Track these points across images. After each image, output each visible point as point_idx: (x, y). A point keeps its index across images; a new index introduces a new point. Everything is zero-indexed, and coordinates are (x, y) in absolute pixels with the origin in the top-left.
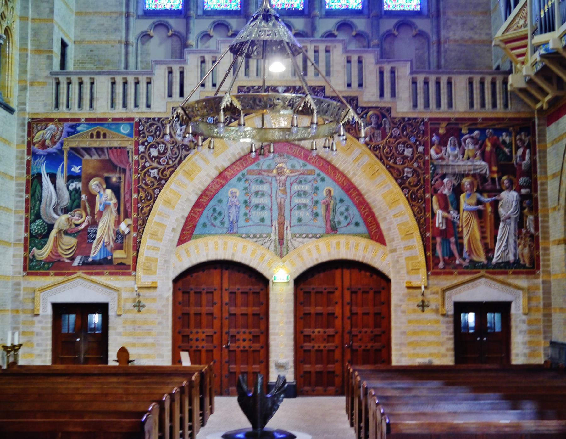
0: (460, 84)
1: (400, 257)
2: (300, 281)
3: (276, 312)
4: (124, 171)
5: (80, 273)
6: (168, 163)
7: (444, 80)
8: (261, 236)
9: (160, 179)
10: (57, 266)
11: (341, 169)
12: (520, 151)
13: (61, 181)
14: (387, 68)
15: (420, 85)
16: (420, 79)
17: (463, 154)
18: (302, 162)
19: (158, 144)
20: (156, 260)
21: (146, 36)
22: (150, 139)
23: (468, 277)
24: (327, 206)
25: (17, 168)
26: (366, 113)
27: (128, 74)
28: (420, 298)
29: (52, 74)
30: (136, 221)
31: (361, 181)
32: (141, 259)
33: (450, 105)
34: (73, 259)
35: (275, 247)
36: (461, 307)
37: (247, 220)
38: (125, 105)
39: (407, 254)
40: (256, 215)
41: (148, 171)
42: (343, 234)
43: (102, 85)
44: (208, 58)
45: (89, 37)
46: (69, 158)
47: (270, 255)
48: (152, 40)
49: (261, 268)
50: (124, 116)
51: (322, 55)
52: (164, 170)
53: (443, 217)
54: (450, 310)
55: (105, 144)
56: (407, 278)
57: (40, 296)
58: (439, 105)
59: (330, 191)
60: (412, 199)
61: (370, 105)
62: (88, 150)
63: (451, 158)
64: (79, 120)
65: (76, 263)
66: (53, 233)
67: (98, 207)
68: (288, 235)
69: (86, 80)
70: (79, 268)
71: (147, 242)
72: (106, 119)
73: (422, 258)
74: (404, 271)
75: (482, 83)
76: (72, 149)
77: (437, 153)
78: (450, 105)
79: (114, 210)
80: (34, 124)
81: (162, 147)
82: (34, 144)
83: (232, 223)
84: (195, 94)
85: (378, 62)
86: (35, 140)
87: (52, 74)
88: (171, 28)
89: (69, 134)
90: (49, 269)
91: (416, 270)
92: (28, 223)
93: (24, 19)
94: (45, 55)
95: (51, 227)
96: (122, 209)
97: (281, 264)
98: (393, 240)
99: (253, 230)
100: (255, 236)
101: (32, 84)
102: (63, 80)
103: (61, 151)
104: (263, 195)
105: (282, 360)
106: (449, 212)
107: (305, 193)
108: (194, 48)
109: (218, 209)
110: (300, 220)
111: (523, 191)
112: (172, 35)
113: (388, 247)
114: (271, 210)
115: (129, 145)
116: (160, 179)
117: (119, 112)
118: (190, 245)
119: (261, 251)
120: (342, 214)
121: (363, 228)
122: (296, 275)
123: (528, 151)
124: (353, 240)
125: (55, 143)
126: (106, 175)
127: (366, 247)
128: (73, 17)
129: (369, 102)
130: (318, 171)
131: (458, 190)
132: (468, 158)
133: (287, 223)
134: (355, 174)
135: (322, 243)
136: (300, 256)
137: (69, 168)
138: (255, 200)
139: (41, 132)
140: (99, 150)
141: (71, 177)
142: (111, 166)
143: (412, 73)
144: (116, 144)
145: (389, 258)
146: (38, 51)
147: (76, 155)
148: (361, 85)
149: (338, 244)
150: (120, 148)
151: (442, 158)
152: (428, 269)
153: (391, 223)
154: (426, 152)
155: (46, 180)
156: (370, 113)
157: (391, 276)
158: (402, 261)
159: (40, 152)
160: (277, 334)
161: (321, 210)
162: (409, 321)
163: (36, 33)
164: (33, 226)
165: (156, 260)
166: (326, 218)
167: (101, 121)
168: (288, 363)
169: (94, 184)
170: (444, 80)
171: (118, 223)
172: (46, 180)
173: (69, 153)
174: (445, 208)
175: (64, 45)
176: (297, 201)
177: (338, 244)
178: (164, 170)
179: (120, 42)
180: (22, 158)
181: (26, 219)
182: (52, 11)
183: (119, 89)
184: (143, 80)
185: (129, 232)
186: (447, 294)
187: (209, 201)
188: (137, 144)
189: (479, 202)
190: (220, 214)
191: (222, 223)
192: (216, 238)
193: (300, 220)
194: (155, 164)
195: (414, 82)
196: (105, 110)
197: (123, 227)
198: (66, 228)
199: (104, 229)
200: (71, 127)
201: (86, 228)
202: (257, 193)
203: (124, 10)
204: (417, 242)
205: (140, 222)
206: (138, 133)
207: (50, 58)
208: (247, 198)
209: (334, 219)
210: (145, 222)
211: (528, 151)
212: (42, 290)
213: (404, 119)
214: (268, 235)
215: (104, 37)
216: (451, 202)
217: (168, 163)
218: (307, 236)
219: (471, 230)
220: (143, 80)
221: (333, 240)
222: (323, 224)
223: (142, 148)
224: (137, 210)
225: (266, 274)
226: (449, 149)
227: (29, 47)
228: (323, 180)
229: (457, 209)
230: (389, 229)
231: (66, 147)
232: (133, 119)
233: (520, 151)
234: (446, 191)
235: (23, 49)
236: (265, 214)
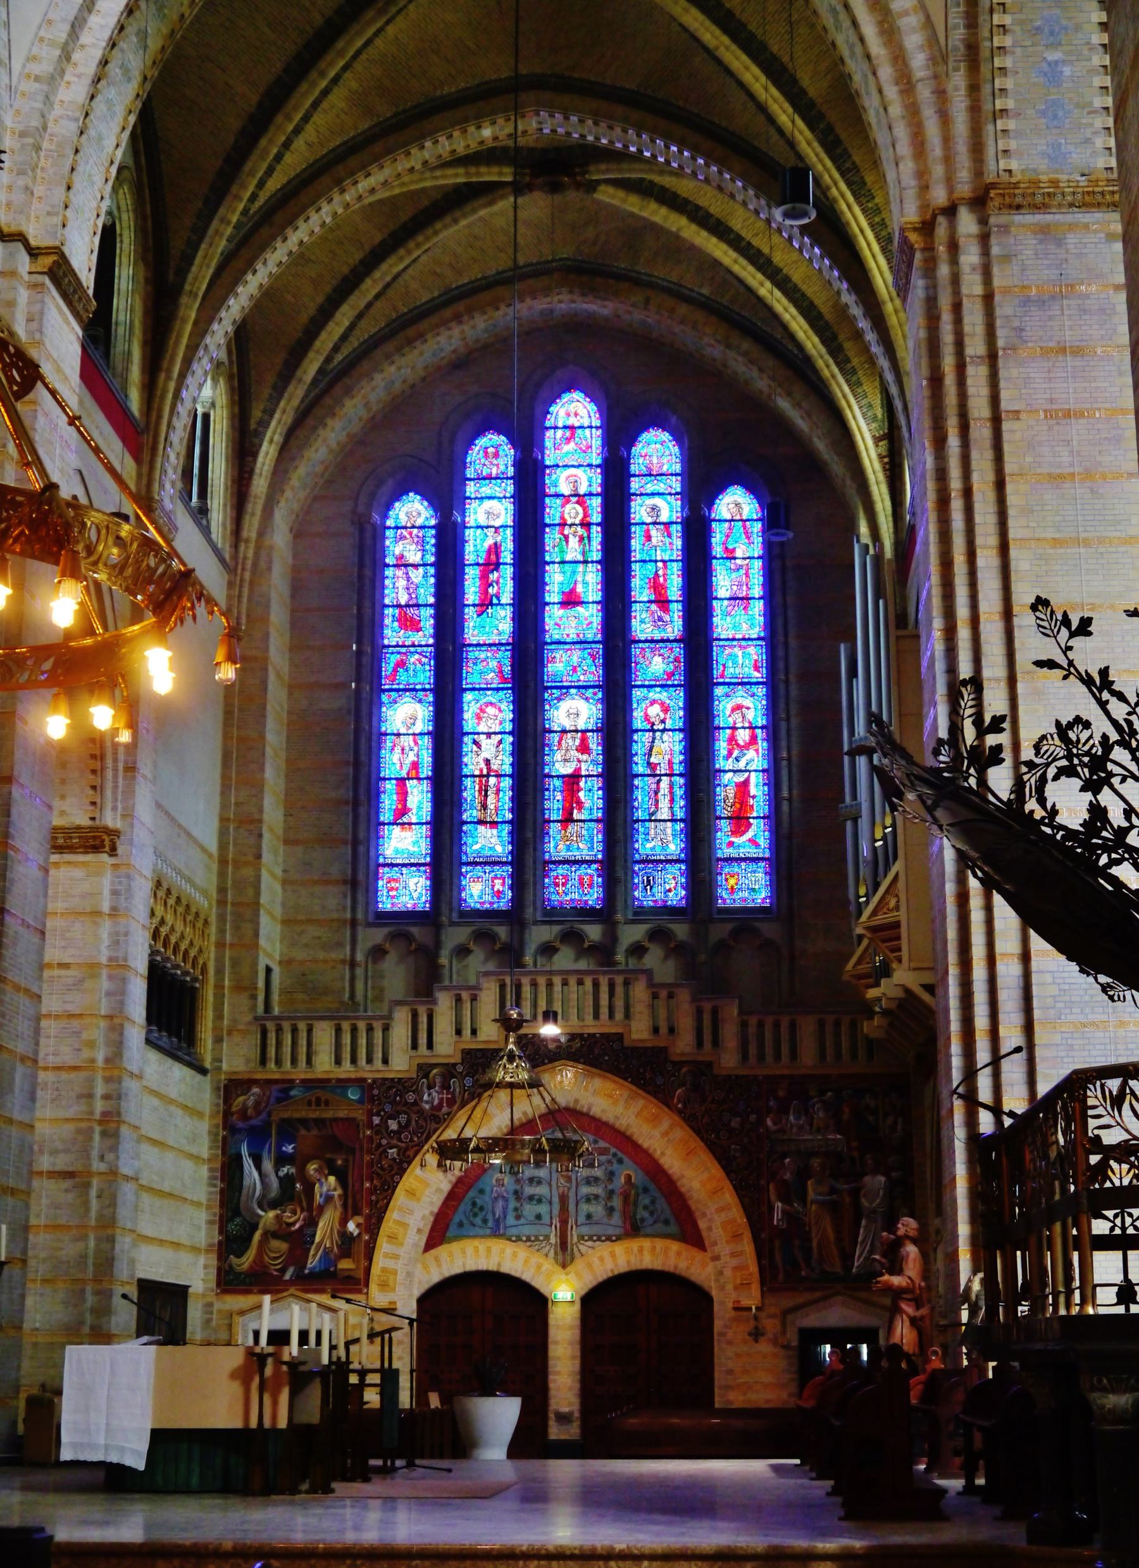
0: (808, 1026)
1: (724, 1266)
2: (593, 1301)
3: (557, 1343)
4: (352, 1151)
5: (292, 1290)
6: (411, 1140)
7: (785, 1022)
8: (537, 1239)
9: (402, 1162)
10: (261, 1281)
11: (645, 1146)
12: (890, 1120)
13: (268, 1165)
14: (707, 1006)
15: (752, 1030)
16: (753, 1021)
17: (811, 1125)
18: (591, 1138)
19: (399, 1113)
20: (395, 1273)
21: (378, 953)
22: (388, 1108)
23: (818, 1294)
24: (626, 1197)
25: (210, 1148)
26: (679, 1071)
27: (357, 1018)
28: (752, 1323)
29: (256, 1019)
30: (368, 1218)
31: (672, 1161)
32: (375, 1271)
33: (794, 1055)
34: (283, 1271)
35: (556, 1253)
36: (812, 1337)
37: (518, 1217)
38: (354, 1060)
39: (734, 1262)
40: (529, 1210)
41: (385, 1151)
42: (646, 1236)
43: (324, 1034)
44: (465, 995)
45: (300, 955)
46: (278, 1133)
47: (548, 1265)
48: (388, 957)
49: (538, 1283)
50: (353, 1076)
51: (619, 990)
52: (407, 1149)
53: (783, 1212)
54: (793, 1338)
55: (329, 1114)
56: (734, 1296)
57: (239, 1320)
58: (778, 1056)
59: (629, 1177)
60: (740, 1189)
61: (684, 1059)
62: (304, 1122)
63: (794, 1130)
64: (292, 1081)
65: (287, 1277)
66: (257, 1236)
67: (318, 1199)
68: (573, 1236)
69: (302, 1026)
70: (291, 1283)
71: (383, 1246)
72: (328, 1080)
73: (754, 1268)
74: (729, 1287)
75: (837, 1024)
76: (283, 1120)
77: (775, 1124)
78: (794, 1055)
79: (338, 1203)
80: (232, 1088)
81: (403, 1118)
82: (232, 1114)
83: (497, 1222)
84: (446, 1047)
85: (694, 1000)
86: (234, 1109)
87: (256, 1019)
88: (415, 940)
89: (279, 1100)
90: (251, 1284)
91: (744, 1285)
92: (223, 1223)
93: (220, 945)
94: (246, 994)
95: (255, 1227)
96: (350, 1202)
97: (563, 1277)
98: (715, 1244)
99: (526, 1230)
100: (528, 1239)
101: (230, 1033)
102: (271, 1026)
103: (267, 1124)
104: (539, 1183)
105: (565, 1409)
106: (791, 1205)
107: (596, 1179)
108: (447, 983)
109: (479, 1202)
110: (589, 1216)
111: (894, 1174)
112: (416, 950)
113: (709, 1254)
114: (550, 1203)
115: (360, 1115)
116: (402, 1162)
117: (346, 1070)
118: (442, 1251)
119: (536, 1259)
120: (645, 1208)
121: (673, 1228)
122: (583, 1293)
123: (900, 1120)
124: (660, 1243)
125: (259, 1113)
126: (328, 1156)
127: (679, 1254)
128: (279, 927)
129: (682, 1054)
130: (613, 1150)
131: (803, 1174)
132: (818, 1130)
133: (571, 1221)
134: (663, 1154)
135: (619, 1248)
136: (589, 1265)
137: (279, 1146)
138: (529, 1190)
139: (241, 1099)
140: (320, 1122)
141: (281, 1160)
142: (337, 1145)
143: (740, 1013)
144: (342, 1114)
145: (710, 1269)
146: (238, 988)
147: (288, 1130)
148: (672, 1030)
149: (641, 1250)
150: (347, 1119)
151: (782, 1131)
152: (763, 1283)
153: (711, 1220)
154: (761, 1122)
155: (248, 1164)
156: (684, 1070)
157: (714, 1293)
158: (728, 1272)
159: (240, 1125)
160: (558, 1373)
161: (617, 1202)
162: (738, 1355)
163: (235, 963)
164: (231, 1227)
165: (395, 1273)
166: (624, 1213)
167: (322, 1083)
168: (571, 1413)
169: (312, 1168)
170: (785, 1022)
171: (344, 1222)
172: (248, 1164)
173: (279, 1128)
174: (785, 1199)
175: (269, 970)
176: (585, 1190)
177: (641, 1250)
178: (407, 1149)
179: (343, 962)
180: (217, 1134)
181: (221, 1216)
182: (256, 934)
183: (347, 1039)
184: (378, 1026)
185: (360, 1234)
186: (789, 1317)
187: (467, 1192)
188: (370, 1114)
189: (833, 1191)
190: (482, 1209)
191: (485, 1221)
192: (476, 1242)
193: (589, 1216)
194: (394, 1142)
195: (744, 1025)
196: (327, 1067)
197: (351, 1226)
198: (273, 1228)
199: (325, 1229)
200: (283, 1091)
201: (301, 1227)
202: (531, 1180)
203: (348, 915)
204: (747, 1247)
205: (373, 1220)
206: (372, 1099)
207: (254, 997)
208: (518, 1187)
209: (635, 1214)
210: (380, 1220)
211: (900, 1120)
212: (242, 1313)
213: (729, 1076)
214: (547, 1237)
215: (321, 955)
216: (793, 1193)
217: (411, 1140)
218: (599, 1239)
219: (822, 1230)
220: (378, 1026)
221: (634, 1244)
222: (620, 1223)
223: (376, 1120)
224: (371, 1204)
225: (544, 1290)
226: (792, 1118)
227: (227, 983)
228: (620, 1161)
229: (803, 1199)
230: (710, 1229)
231: (275, 1118)
232: (365, 1080)
233: (890, 1120)
234: (787, 1176)
235: (219, 987)
236: (543, 1209)
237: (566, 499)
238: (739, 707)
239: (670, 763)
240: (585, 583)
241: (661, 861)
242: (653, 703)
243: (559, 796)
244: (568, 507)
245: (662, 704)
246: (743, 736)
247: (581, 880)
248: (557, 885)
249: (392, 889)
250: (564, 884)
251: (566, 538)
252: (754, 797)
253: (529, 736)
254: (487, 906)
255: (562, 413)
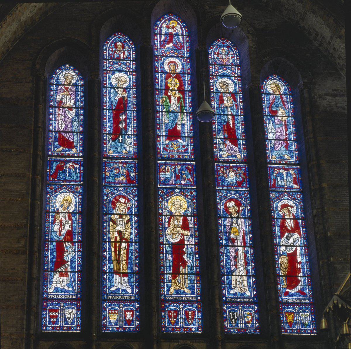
237: (168, 76)
238: (285, 206)
239: (244, 239)
240: (183, 125)
241: (240, 303)
242: (230, 200)
243: (170, 257)
244: (169, 80)
245: (236, 201)
246: (290, 224)
247: (187, 314)
248: (170, 317)
249: (53, 317)
250: (175, 317)
251: (170, 98)
252: (300, 263)
253: (149, 219)
254: (121, 330)
255: (164, 26)
